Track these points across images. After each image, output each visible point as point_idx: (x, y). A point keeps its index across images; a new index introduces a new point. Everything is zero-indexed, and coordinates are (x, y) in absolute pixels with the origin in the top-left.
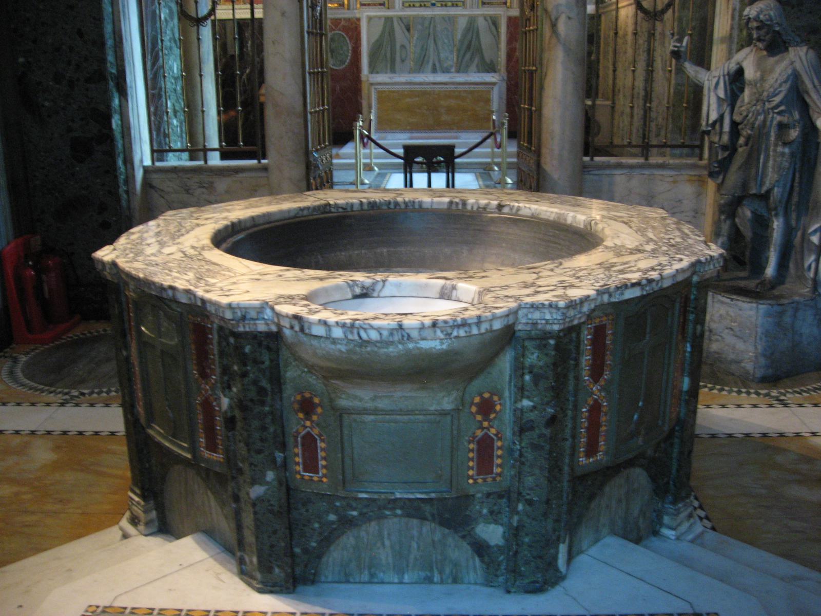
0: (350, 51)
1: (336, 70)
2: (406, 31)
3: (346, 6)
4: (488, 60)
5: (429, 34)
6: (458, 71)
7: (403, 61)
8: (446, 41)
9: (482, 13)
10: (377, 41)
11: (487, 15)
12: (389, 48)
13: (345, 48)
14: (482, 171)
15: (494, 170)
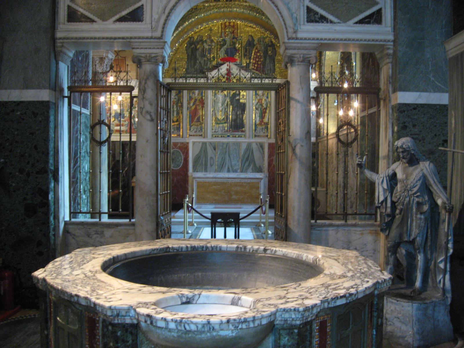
2: (213, 149)
3: (181, 136)
6: (242, 171)
8: (235, 155)
9: (254, 141)
10: (197, 155)
13: (180, 158)
14: (254, 226)
15: (261, 226)
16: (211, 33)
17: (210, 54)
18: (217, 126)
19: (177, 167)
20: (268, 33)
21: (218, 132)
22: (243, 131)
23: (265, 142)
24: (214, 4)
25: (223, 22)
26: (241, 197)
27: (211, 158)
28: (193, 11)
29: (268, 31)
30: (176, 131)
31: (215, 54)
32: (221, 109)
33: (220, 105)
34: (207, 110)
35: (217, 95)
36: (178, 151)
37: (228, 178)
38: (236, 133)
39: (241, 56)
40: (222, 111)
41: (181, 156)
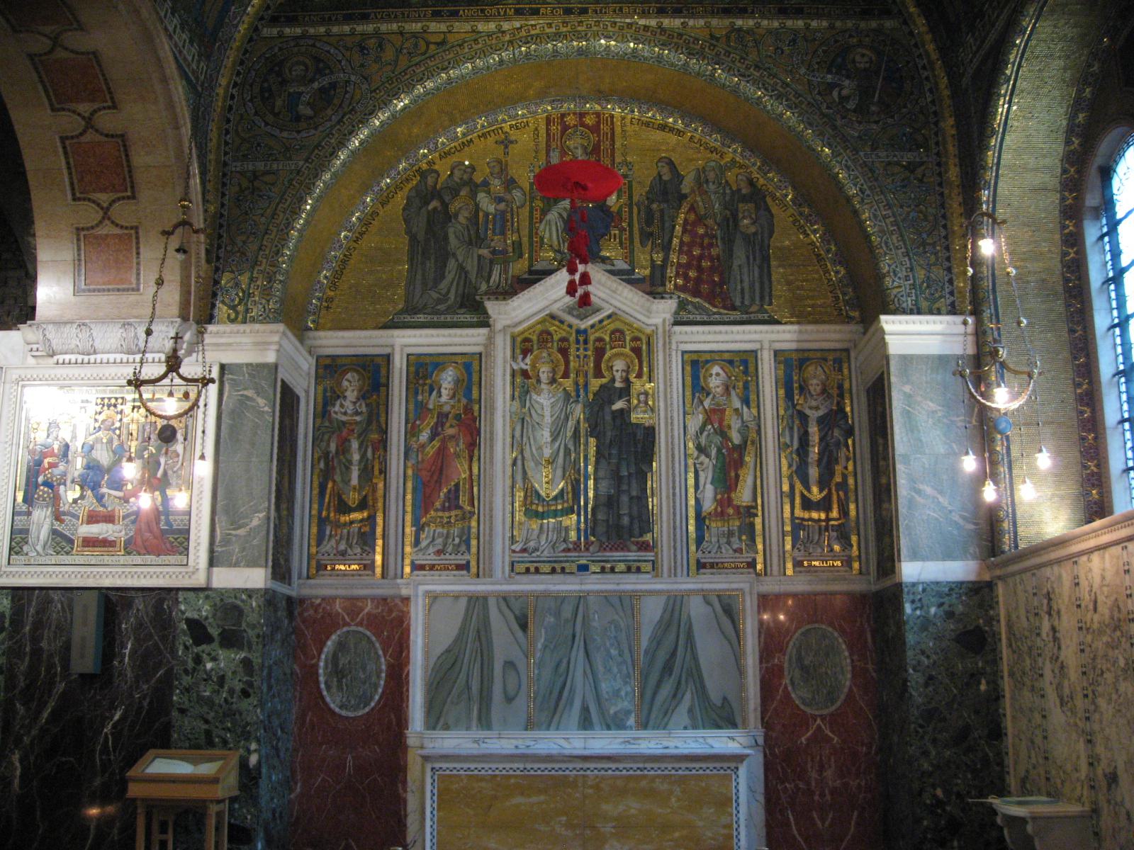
0: (383, 675)
1: (347, 718)
2: (516, 627)
3: (378, 570)
4: (715, 696)
5: (574, 637)
6: (644, 725)
7: (509, 699)
8: (614, 652)
9: (699, 586)
10: (448, 651)
11: (711, 590)
12: (478, 665)
13: (371, 667)
16: (506, 154)
17: (503, 233)
18: (535, 525)
19: (356, 708)
20: (735, 151)
21: (536, 550)
22: (645, 547)
24: (517, 24)
25: (555, 114)
27: (510, 665)
28: (430, 52)
29: (733, 141)
30: (359, 550)
31: (525, 232)
32: (547, 452)
33: (546, 435)
34: (492, 458)
35: (535, 397)
36: (364, 634)
38: (618, 555)
39: (632, 242)
40: (551, 462)
41: (379, 656)
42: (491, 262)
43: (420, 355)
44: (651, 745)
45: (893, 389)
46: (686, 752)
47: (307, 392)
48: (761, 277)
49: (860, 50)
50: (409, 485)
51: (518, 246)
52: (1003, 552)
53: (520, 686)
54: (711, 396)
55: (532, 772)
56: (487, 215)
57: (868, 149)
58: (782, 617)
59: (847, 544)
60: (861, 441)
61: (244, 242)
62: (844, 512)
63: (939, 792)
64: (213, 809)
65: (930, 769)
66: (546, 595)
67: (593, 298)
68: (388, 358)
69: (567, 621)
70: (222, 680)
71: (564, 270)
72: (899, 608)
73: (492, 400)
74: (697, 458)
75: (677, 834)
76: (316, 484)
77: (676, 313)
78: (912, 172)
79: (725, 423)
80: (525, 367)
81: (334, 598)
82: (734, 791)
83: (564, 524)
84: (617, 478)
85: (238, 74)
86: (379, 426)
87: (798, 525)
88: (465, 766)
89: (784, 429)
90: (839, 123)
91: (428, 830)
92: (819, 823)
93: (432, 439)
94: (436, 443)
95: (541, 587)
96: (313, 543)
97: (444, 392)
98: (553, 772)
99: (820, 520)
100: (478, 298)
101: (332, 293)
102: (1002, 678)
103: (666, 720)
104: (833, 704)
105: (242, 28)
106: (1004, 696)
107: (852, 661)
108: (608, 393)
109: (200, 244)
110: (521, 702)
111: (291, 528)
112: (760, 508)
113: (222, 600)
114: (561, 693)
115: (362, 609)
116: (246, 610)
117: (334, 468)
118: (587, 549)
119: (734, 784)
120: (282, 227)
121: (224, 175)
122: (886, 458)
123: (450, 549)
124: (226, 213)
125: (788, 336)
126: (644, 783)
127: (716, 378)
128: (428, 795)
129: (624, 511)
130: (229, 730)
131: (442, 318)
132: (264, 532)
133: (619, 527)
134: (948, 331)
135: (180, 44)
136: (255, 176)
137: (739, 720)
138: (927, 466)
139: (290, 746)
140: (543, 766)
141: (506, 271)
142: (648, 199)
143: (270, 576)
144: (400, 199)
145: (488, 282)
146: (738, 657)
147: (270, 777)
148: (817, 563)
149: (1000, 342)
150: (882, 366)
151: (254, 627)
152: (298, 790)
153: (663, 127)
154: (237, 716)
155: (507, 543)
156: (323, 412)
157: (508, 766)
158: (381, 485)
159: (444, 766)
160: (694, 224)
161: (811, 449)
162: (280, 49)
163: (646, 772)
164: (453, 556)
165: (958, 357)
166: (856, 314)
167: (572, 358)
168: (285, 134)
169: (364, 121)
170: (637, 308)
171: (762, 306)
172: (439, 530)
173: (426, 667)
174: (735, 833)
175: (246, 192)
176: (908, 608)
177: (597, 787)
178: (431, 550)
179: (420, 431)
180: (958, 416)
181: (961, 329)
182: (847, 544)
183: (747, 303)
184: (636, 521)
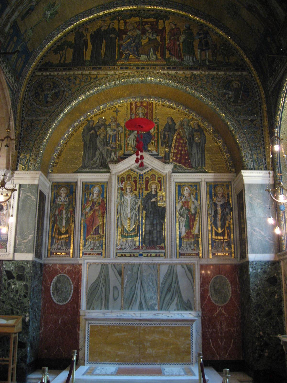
0: (72, 291)
1: (60, 305)
4: (185, 299)
5: (137, 278)
6: (161, 309)
7: (115, 299)
8: (151, 284)
9: (180, 262)
10: (94, 283)
13: (68, 287)
17: (115, 141)
18: (124, 240)
19: (63, 301)
20: (193, 115)
21: (125, 248)
22: (162, 248)
23: (194, 263)
24: (121, 72)
25: (133, 102)
26: (161, 351)
28: (92, 81)
29: (193, 111)
30: (65, 248)
31: (123, 141)
32: (129, 215)
33: (129, 210)
34: (110, 217)
35: (125, 197)
36: (66, 277)
37: (140, 320)
38: (152, 251)
39: (158, 145)
40: (130, 219)
41: (71, 285)
42: (111, 151)
43: (86, 182)
44: (163, 316)
45: (246, 195)
46: (175, 318)
47: (48, 194)
48: (202, 156)
49: (234, 82)
50: (82, 226)
51: (120, 146)
52: (283, 251)
53: (118, 295)
54: (184, 197)
55: (122, 325)
56: (110, 135)
57: (237, 115)
58: (209, 272)
59: (230, 248)
60: (235, 213)
61: (28, 143)
62: (229, 237)
63: (261, 333)
64: (13, 336)
65: (258, 325)
66: (128, 264)
67: (144, 163)
68: (76, 183)
69: (135, 273)
70: (17, 292)
71: (135, 154)
72: (248, 270)
73: (111, 198)
74: (180, 218)
75: (171, 347)
76: (51, 225)
77: (173, 169)
78: (252, 122)
79: (189, 206)
80: (122, 187)
81: (56, 264)
82: (191, 332)
83: (134, 240)
84: (153, 225)
85: (28, 87)
86: (73, 206)
87: (213, 241)
88: (99, 322)
89: (209, 208)
90: (228, 106)
91: (86, 344)
92: (220, 343)
93: (90, 210)
94: (92, 212)
95: (126, 261)
96: (49, 245)
97: (95, 195)
98: (129, 325)
99: (221, 239)
100: (106, 163)
101: (57, 161)
102: (283, 294)
103: (168, 307)
104: (225, 302)
105: (29, 72)
106: (283, 300)
107: (232, 288)
108: (150, 196)
109: (13, 144)
110: (119, 301)
111: (42, 240)
112: (201, 235)
113: (18, 264)
114: (133, 297)
115: (66, 268)
116: (26, 267)
117: (57, 220)
118: (142, 249)
119: (191, 330)
120: (41, 138)
121: (22, 121)
122: (243, 218)
123: (96, 248)
124: (22, 134)
125: (210, 177)
126: (160, 329)
127: (186, 191)
128: (87, 332)
129: (155, 236)
130: (19, 309)
131: (94, 170)
132: (33, 241)
133: (153, 241)
134: (264, 176)
135: (8, 77)
136: (32, 121)
137: (193, 307)
138: (257, 221)
139: (40, 314)
140: (126, 323)
141: (116, 154)
142: (164, 130)
143: (34, 257)
144: (81, 130)
145: (110, 158)
146: (193, 286)
147: (33, 325)
148: (220, 254)
149: (282, 180)
150: (242, 188)
151: (28, 273)
152: (42, 330)
153: (169, 107)
154: (22, 304)
155: (115, 246)
156: (54, 201)
157: (114, 322)
158: (73, 226)
159: (92, 322)
160: (179, 139)
161: (218, 215)
162: (42, 79)
163: (161, 325)
164: (97, 250)
165: (267, 185)
166: (233, 170)
167: (138, 184)
168: (43, 108)
169: (69, 103)
170: (160, 167)
171: (202, 167)
172: (92, 241)
173: (87, 288)
174: (191, 347)
175: (29, 127)
176: (251, 270)
177: (144, 330)
178: (89, 248)
179: (86, 208)
180: (268, 204)
181: (268, 175)
182: (230, 248)
183: (197, 166)
184: (159, 239)
